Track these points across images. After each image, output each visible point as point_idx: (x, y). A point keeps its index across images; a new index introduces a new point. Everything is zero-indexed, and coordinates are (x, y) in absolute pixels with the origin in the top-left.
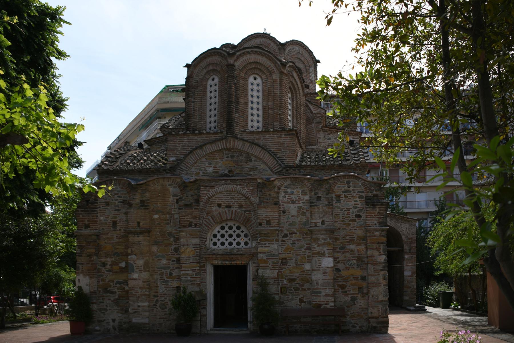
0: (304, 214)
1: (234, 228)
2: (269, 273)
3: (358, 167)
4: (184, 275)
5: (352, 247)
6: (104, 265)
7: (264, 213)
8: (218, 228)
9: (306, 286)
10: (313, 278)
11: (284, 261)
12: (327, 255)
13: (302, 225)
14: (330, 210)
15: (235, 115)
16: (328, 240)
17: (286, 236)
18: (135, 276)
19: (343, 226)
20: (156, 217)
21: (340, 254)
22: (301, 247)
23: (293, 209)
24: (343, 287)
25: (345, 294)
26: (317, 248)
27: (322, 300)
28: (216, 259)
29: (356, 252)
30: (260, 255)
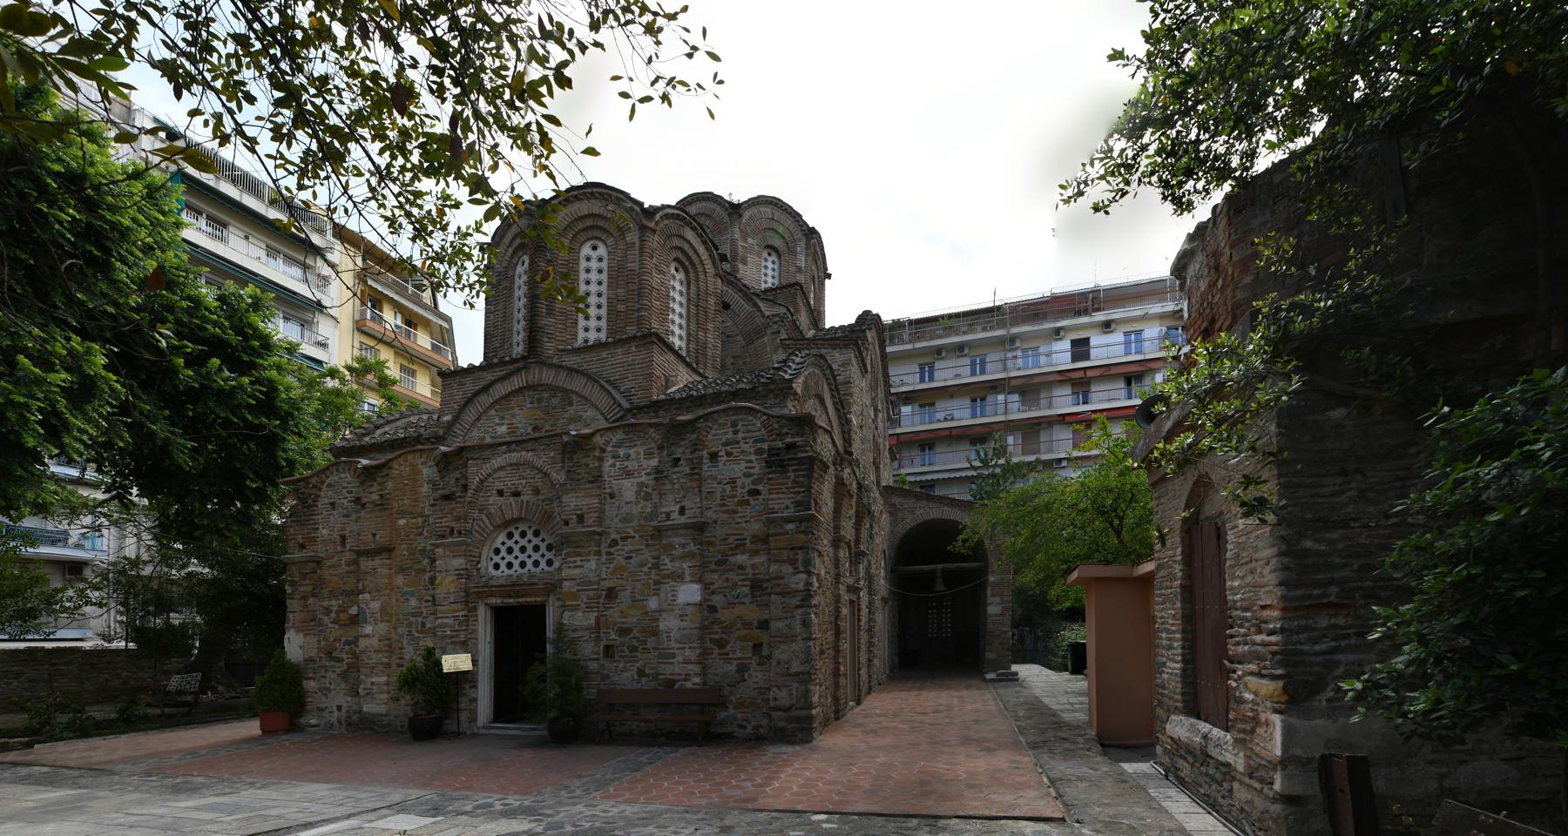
0: (648, 497)
1: (530, 535)
2: (580, 619)
3: (771, 391)
4: (441, 626)
5: (741, 559)
6: (327, 611)
7: (572, 501)
8: (502, 537)
9: (651, 643)
10: (662, 626)
11: (611, 593)
12: (688, 578)
13: (646, 519)
14: (695, 484)
15: (545, 321)
16: (692, 547)
17: (614, 543)
18: (368, 629)
19: (724, 516)
20: (402, 522)
21: (716, 576)
22: (643, 565)
23: (628, 489)
24: (721, 644)
25: (726, 657)
26: (668, 564)
27: (677, 671)
28: (492, 595)
29: (749, 570)
30: (567, 584)
